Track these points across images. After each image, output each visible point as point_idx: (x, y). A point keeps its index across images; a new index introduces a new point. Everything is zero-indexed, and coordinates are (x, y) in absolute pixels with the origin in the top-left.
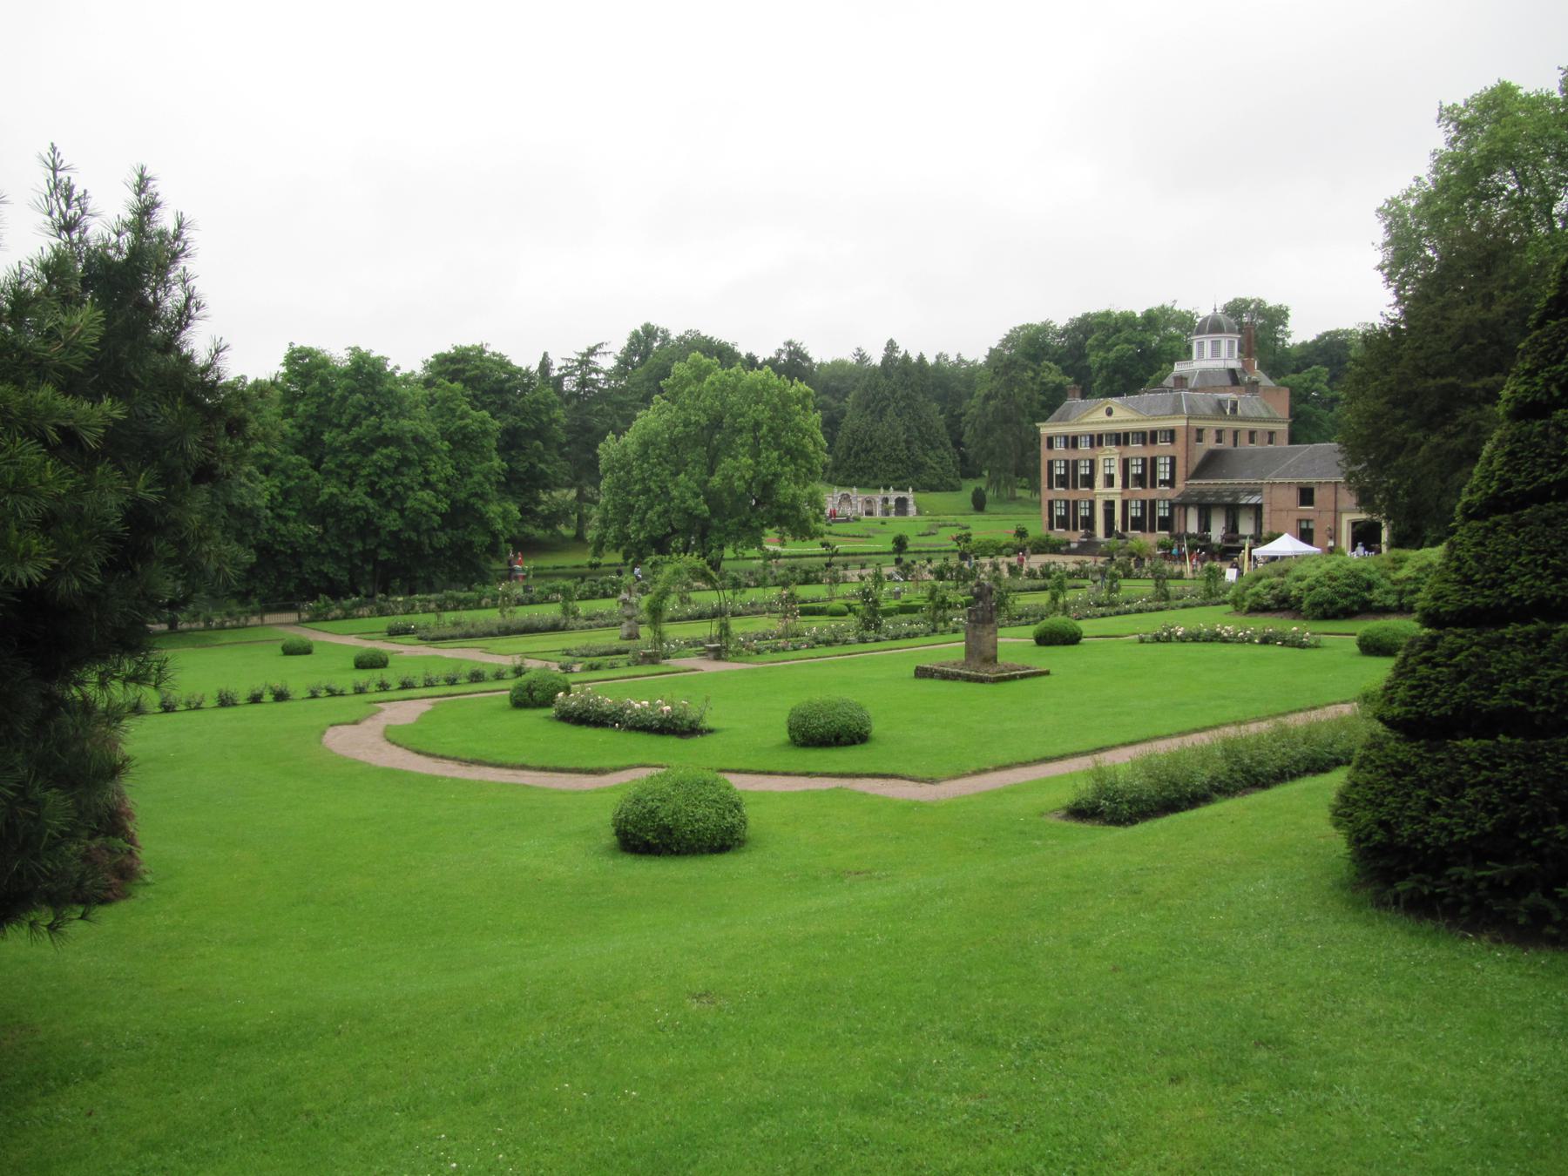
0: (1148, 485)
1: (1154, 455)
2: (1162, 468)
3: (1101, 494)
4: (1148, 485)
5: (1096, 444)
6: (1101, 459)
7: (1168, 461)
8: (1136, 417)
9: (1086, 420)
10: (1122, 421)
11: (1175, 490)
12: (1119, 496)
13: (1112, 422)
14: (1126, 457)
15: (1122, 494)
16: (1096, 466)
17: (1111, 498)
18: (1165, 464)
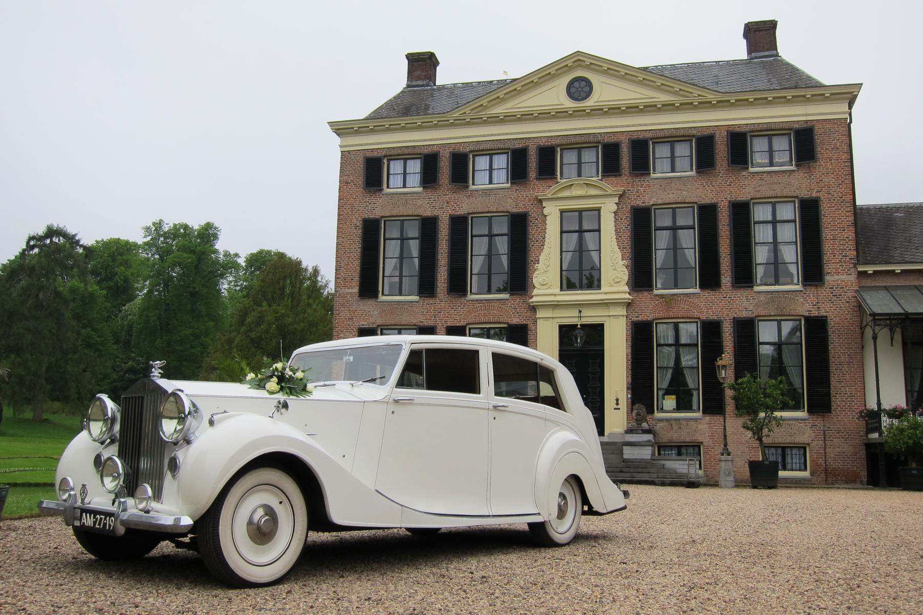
0: (726, 278)
1: (743, 197)
2: (762, 234)
3: (555, 306)
4: (726, 278)
5: (532, 174)
6: (552, 211)
7: (787, 212)
8: (664, 98)
9: (499, 110)
10: (632, 109)
11: (823, 292)
12: (624, 312)
13: (598, 112)
14: (639, 203)
15: (629, 305)
16: (532, 231)
17: (591, 317)
18: (774, 222)
